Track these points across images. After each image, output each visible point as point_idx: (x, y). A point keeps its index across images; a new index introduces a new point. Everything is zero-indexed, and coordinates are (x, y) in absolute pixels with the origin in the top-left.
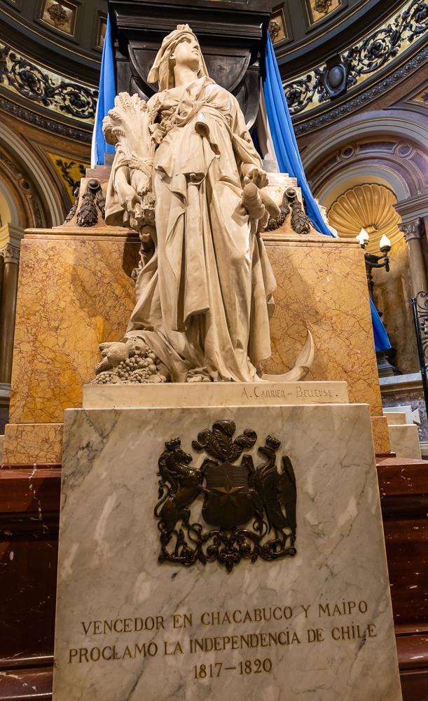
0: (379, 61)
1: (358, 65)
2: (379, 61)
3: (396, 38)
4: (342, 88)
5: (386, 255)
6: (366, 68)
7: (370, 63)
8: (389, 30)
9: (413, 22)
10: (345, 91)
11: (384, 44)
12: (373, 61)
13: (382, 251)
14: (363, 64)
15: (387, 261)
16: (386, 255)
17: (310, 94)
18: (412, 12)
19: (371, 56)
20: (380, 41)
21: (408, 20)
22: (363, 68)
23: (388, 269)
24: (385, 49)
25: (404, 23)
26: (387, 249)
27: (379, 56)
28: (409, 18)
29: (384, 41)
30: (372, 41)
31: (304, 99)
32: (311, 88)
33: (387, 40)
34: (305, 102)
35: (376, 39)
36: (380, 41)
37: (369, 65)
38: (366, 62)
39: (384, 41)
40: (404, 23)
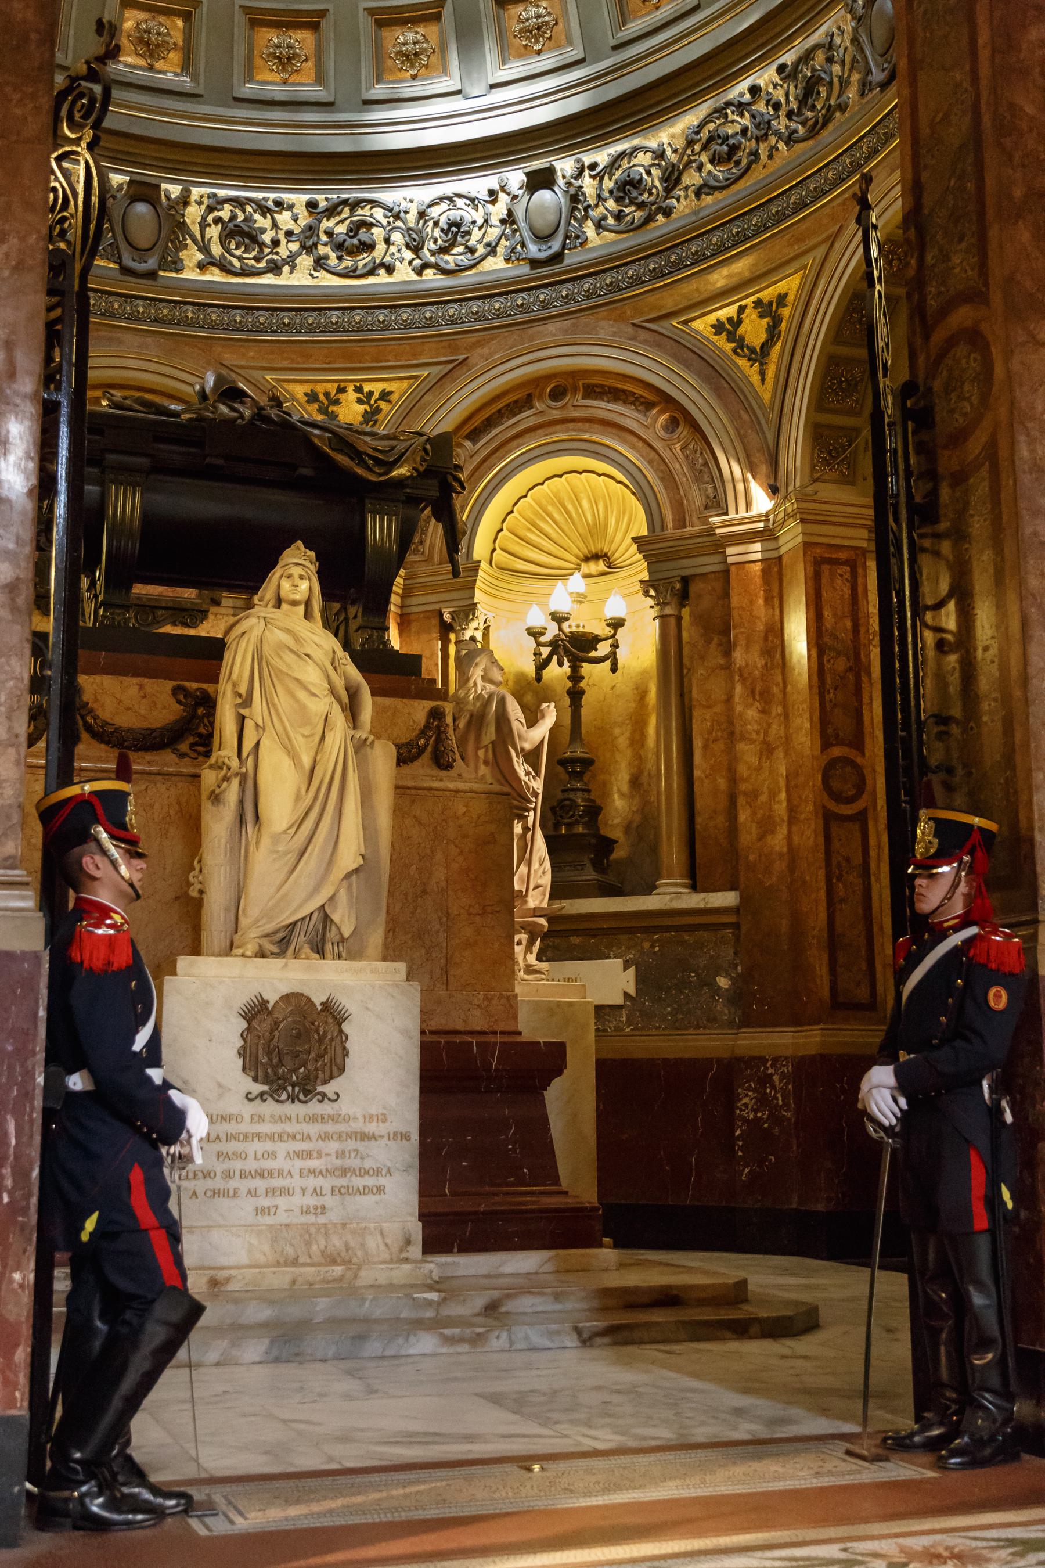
0: (639, 215)
1: (597, 206)
2: (639, 215)
3: (672, 178)
4: (556, 245)
5: (613, 636)
6: (611, 221)
7: (621, 211)
8: (659, 155)
9: (704, 158)
10: (557, 258)
11: (649, 180)
12: (627, 210)
13: (608, 625)
14: (606, 209)
15: (615, 646)
16: (613, 636)
17: (493, 233)
18: (704, 135)
19: (623, 198)
20: (641, 170)
21: (697, 147)
22: (605, 218)
23: (614, 669)
24: (651, 194)
25: (689, 152)
26: (617, 624)
27: (641, 206)
28: (697, 147)
29: (649, 173)
30: (625, 164)
31: (480, 242)
32: (494, 221)
33: (656, 172)
34: (481, 250)
35: (635, 161)
36: (641, 170)
37: (619, 216)
38: (611, 204)
39: (649, 173)
40: (689, 152)
